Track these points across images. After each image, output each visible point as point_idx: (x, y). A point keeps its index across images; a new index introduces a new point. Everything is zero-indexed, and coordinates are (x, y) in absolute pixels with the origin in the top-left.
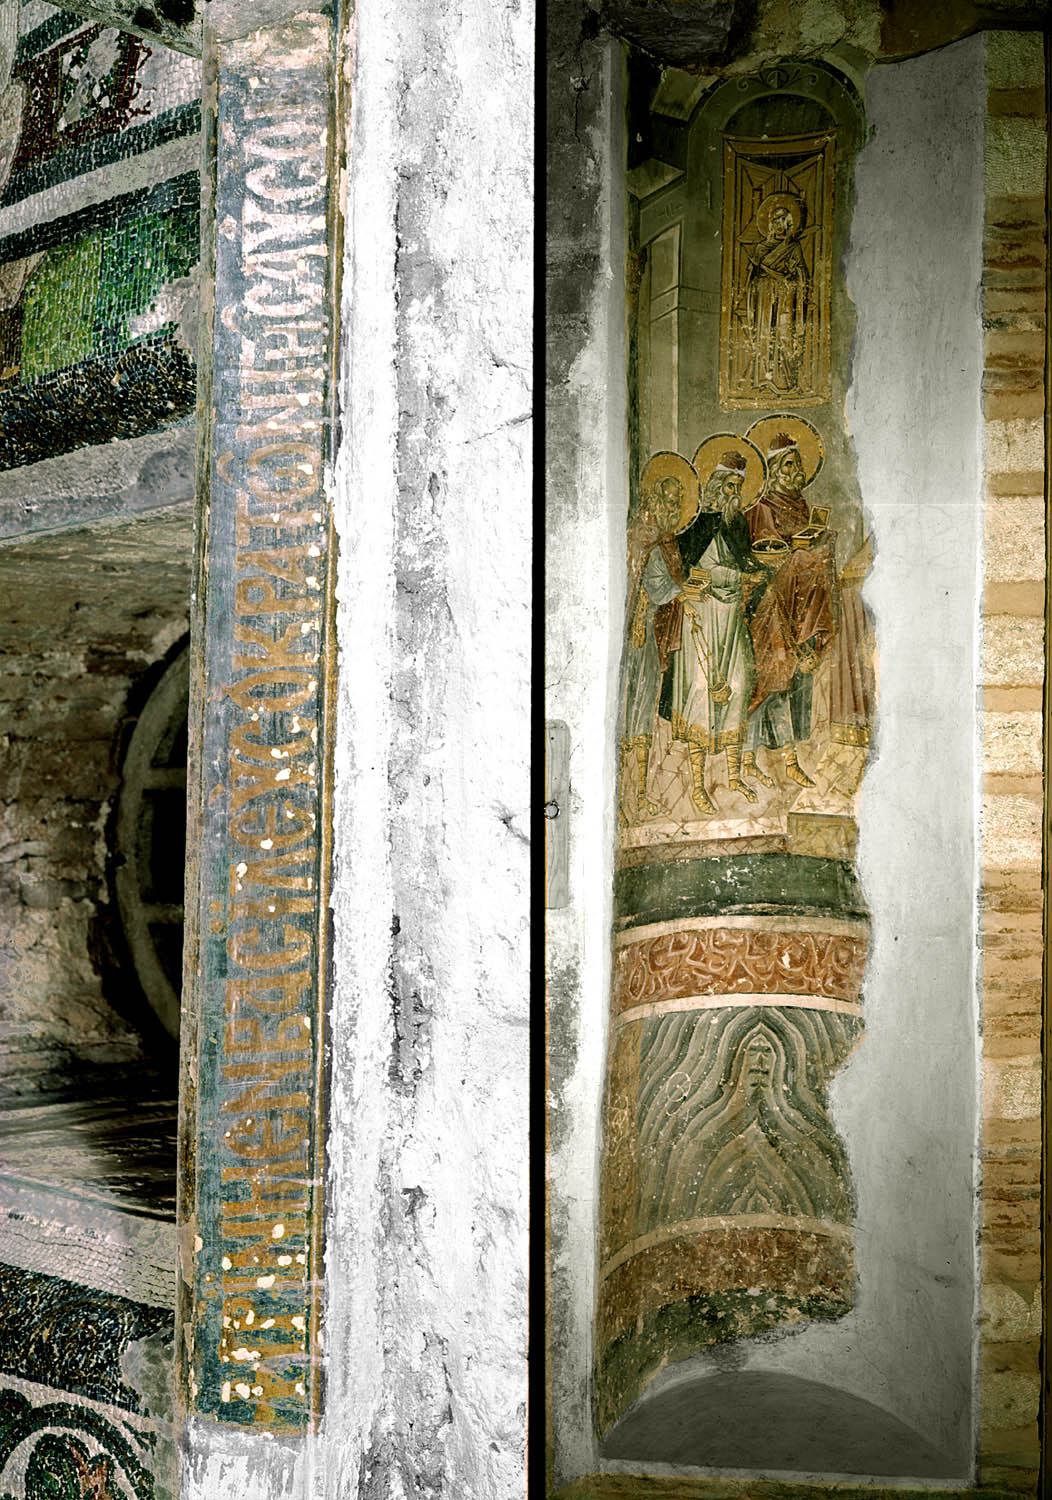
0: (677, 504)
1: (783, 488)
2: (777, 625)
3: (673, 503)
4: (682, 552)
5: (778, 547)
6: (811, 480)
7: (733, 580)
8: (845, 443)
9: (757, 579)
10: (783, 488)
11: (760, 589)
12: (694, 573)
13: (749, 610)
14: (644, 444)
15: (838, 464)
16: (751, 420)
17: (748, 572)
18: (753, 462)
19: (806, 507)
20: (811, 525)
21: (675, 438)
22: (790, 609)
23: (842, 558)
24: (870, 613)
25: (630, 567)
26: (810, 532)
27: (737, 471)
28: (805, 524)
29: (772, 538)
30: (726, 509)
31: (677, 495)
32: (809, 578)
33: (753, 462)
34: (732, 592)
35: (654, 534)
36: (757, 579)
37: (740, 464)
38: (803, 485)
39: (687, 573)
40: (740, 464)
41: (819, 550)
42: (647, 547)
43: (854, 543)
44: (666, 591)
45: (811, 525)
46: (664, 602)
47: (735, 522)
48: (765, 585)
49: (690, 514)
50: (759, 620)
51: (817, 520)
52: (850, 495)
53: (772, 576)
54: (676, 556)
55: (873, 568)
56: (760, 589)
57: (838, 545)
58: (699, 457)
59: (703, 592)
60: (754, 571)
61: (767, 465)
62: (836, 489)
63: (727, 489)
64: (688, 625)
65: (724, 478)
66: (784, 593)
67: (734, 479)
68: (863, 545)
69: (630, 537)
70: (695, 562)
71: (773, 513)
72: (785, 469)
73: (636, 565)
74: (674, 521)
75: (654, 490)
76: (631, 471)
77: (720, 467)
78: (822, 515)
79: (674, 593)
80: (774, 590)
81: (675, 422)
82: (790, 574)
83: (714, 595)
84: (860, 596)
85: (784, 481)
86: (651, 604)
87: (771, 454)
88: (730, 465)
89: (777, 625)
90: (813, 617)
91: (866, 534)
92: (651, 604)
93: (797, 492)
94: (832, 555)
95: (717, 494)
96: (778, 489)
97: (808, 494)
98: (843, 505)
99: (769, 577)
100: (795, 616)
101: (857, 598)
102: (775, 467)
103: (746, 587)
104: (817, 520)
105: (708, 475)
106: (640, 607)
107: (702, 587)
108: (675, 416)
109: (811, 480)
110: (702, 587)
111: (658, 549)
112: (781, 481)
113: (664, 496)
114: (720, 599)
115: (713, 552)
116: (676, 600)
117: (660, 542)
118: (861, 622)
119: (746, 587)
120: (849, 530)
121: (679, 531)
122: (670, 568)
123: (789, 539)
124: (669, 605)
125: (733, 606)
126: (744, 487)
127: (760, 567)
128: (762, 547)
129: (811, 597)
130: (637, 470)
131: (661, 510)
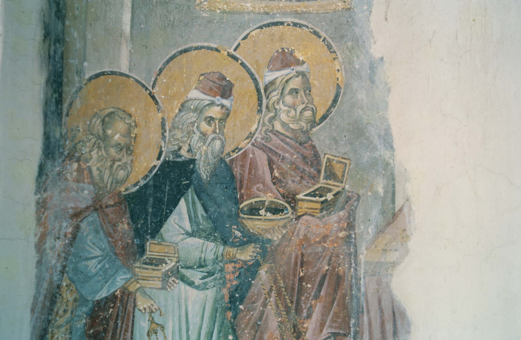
0: (128, 149)
1: (283, 124)
2: (273, 322)
3: (120, 148)
4: (134, 218)
5: (276, 210)
6: (324, 118)
7: (210, 256)
8: (372, 67)
9: (247, 254)
10: (283, 124)
11: (251, 270)
12: (153, 249)
13: (236, 298)
14: (73, 61)
15: (361, 96)
16: (242, 27)
17: (233, 245)
18: (243, 86)
19: (316, 156)
20: (322, 182)
21: (125, 51)
22: (293, 296)
23: (366, 231)
24: (403, 315)
25: (40, 247)
26: (320, 192)
27: (218, 100)
28: (314, 178)
29: (268, 198)
30: (204, 154)
31: (129, 132)
32: (318, 257)
33: (243, 86)
34: (210, 274)
35: (86, 196)
36: (247, 254)
37: (225, 90)
38: (313, 123)
39: (142, 250)
40: (225, 90)
41: (334, 218)
42: (77, 215)
43: (383, 212)
44: (107, 277)
45: (322, 182)
46: (103, 294)
47: (214, 174)
48: (257, 265)
49: (145, 164)
50: (248, 314)
51: (331, 175)
52: (376, 141)
53: (267, 251)
54: (124, 226)
55: (407, 252)
56: (251, 270)
57: (360, 214)
58: (163, 79)
59: (166, 276)
60: (242, 244)
61: (262, 93)
62: (358, 132)
63: (204, 126)
64: (142, 324)
65: (199, 111)
66: (284, 278)
67: (215, 112)
68: (395, 216)
69: (42, 206)
70: (155, 232)
71: (271, 163)
72: (289, 99)
73: (55, 246)
74: (122, 174)
75: (89, 131)
76: (47, 103)
77: (194, 94)
78: (338, 170)
79: (120, 280)
80: (270, 271)
81: (127, 28)
82: (292, 251)
83: (183, 279)
84: (388, 285)
85: (287, 115)
86: (81, 300)
87: (270, 77)
88: (209, 92)
89: (273, 322)
90: (324, 315)
91: (399, 201)
92: (81, 300)
93: (306, 132)
94: (351, 226)
95: (190, 134)
96: (278, 127)
97: (321, 137)
98: (366, 156)
99: (264, 253)
100: (298, 311)
101: (382, 287)
102: (275, 96)
103: (230, 267)
104: (331, 175)
105: (177, 104)
106: (60, 308)
107: (165, 268)
108: (127, 17)
109: (324, 118)
110: (165, 268)
111: (94, 217)
112: (283, 117)
113: (104, 138)
114: (191, 284)
115: (180, 219)
116: (124, 291)
117: (97, 206)
118: (389, 327)
119: (230, 267)
120: (375, 193)
121: (130, 187)
122: (113, 245)
123: (292, 199)
124: (113, 298)
125: (210, 294)
126: (230, 122)
127: (250, 238)
128: (253, 211)
129: (321, 285)
130: (59, 102)
131: (100, 159)
